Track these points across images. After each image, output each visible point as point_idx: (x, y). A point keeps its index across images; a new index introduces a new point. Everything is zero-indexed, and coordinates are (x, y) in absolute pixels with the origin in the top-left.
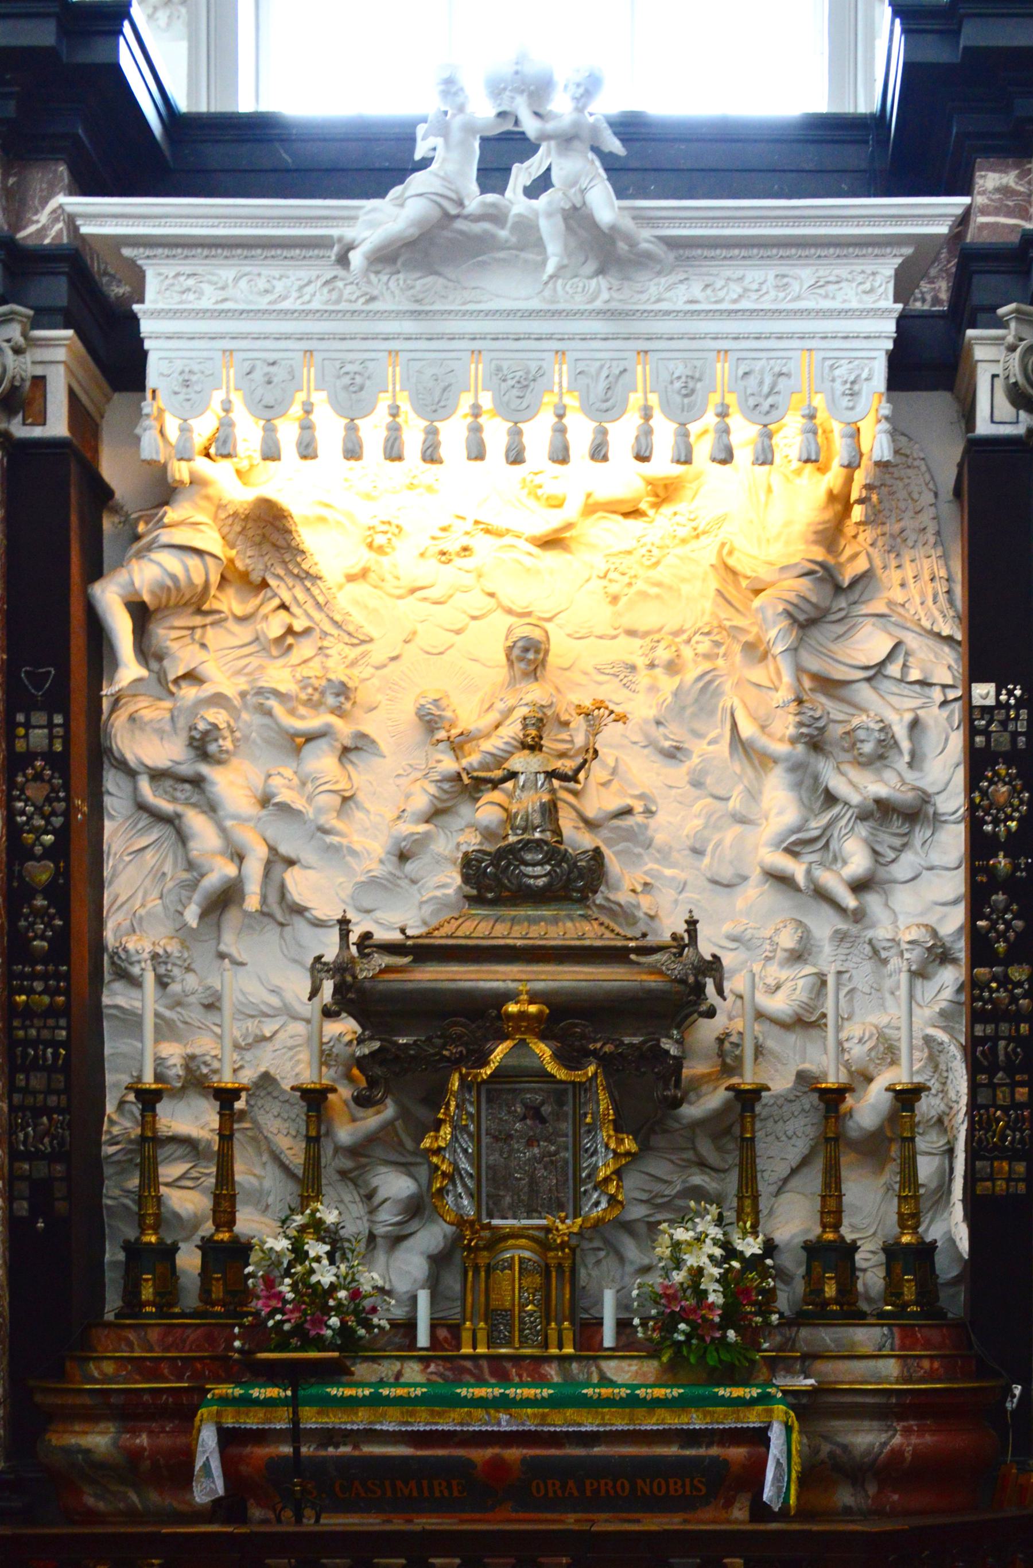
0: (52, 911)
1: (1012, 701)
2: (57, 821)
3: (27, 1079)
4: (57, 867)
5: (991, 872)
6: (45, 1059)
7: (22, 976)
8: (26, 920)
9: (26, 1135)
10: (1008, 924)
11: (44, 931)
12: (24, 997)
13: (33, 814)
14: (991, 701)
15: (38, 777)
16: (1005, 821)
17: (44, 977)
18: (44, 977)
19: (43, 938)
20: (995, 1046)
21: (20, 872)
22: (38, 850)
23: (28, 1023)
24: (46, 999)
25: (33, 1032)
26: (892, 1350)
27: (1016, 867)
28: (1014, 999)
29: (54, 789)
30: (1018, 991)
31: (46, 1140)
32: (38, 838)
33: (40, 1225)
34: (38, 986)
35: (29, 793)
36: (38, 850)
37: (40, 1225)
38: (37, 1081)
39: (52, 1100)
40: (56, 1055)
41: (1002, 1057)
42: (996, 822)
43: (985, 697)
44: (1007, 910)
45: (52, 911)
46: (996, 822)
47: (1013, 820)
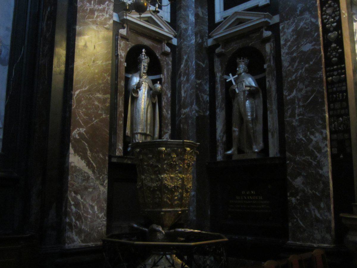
0: (338, 47)
2: (337, 18)
3: (334, 105)
4: (338, 33)
6: (339, 97)
7: (330, 71)
8: (330, 52)
9: (335, 125)
11: (336, 54)
12: (331, 78)
13: (329, 18)
15: (330, 6)
17: (337, 70)
18: (337, 70)
19: (335, 57)
21: (327, 37)
22: (332, 29)
23: (333, 86)
24: (338, 77)
25: (335, 89)
29: (335, 8)
31: (342, 126)
32: (331, 25)
33: (341, 156)
34: (335, 73)
35: (327, 12)
36: (332, 29)
37: (341, 156)
38: (337, 105)
39: (343, 112)
40: (343, 96)
45: (338, 47)
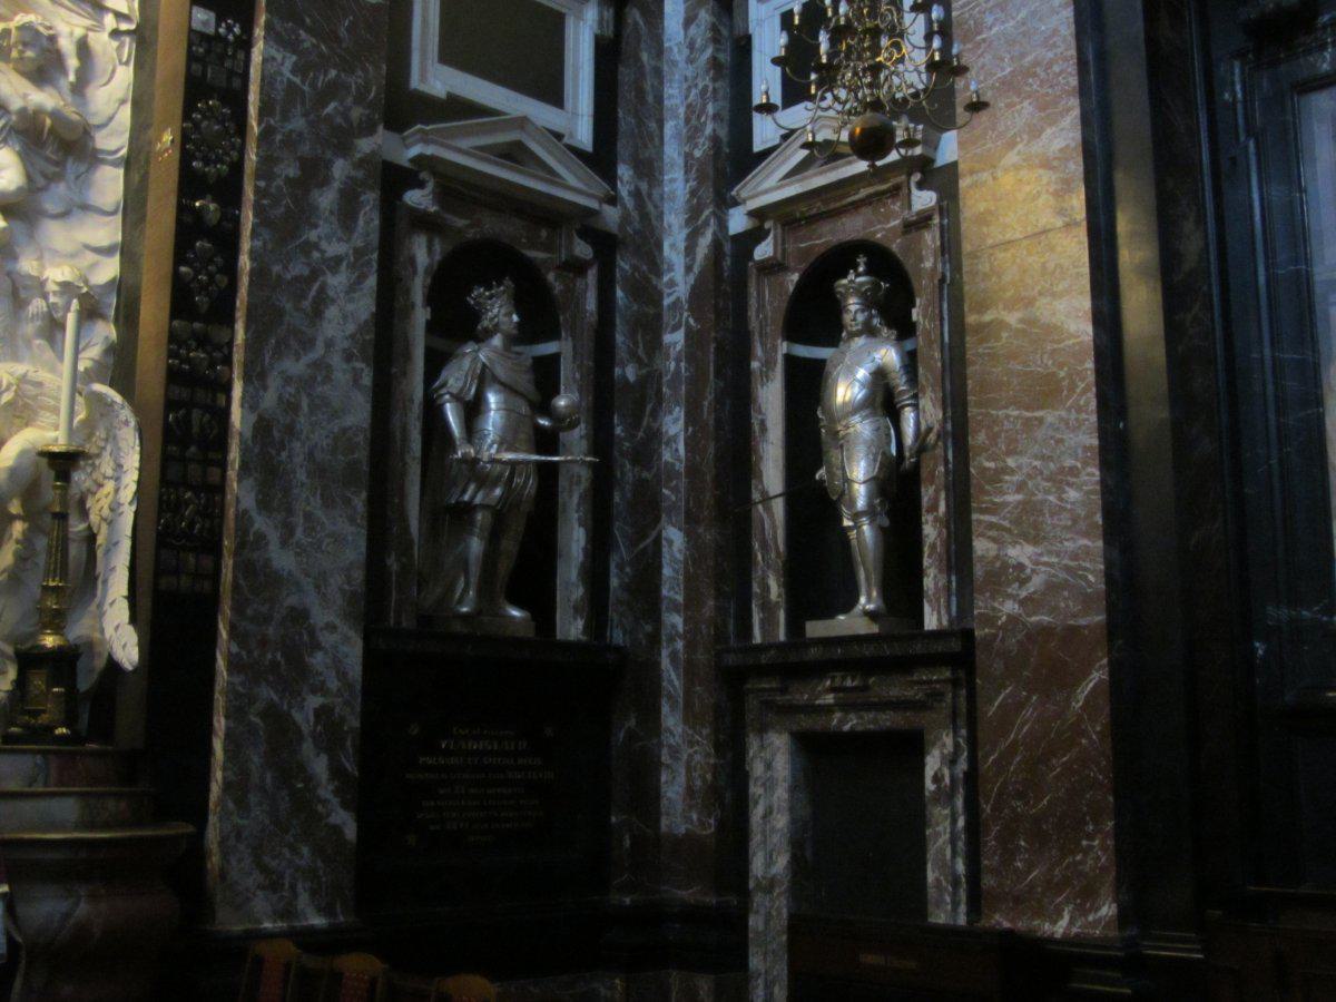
1: (231, 37)
5: (199, 214)
10: (211, 276)
14: (211, 30)
16: (215, 163)
20: (189, 414)
26: (46, 785)
27: (224, 217)
28: (212, 365)
30: (217, 355)
41: (196, 429)
42: (207, 162)
43: (205, 23)
44: (211, 261)
46: (207, 162)
47: (223, 163)
